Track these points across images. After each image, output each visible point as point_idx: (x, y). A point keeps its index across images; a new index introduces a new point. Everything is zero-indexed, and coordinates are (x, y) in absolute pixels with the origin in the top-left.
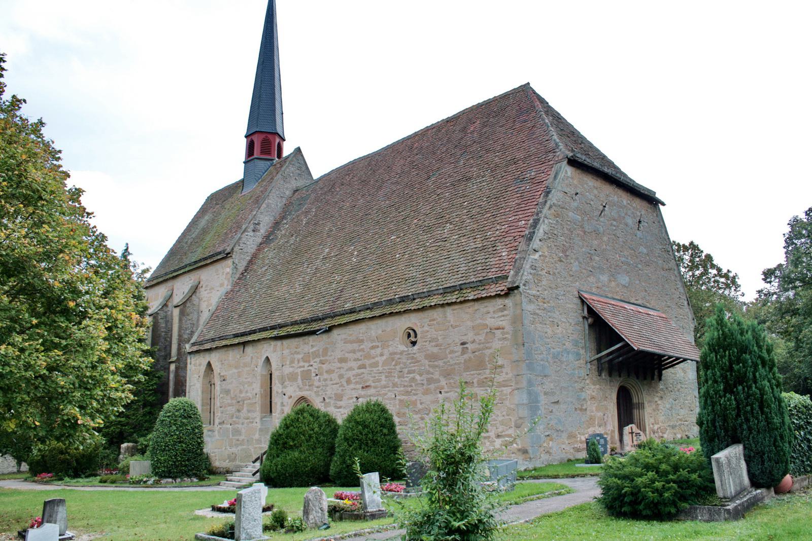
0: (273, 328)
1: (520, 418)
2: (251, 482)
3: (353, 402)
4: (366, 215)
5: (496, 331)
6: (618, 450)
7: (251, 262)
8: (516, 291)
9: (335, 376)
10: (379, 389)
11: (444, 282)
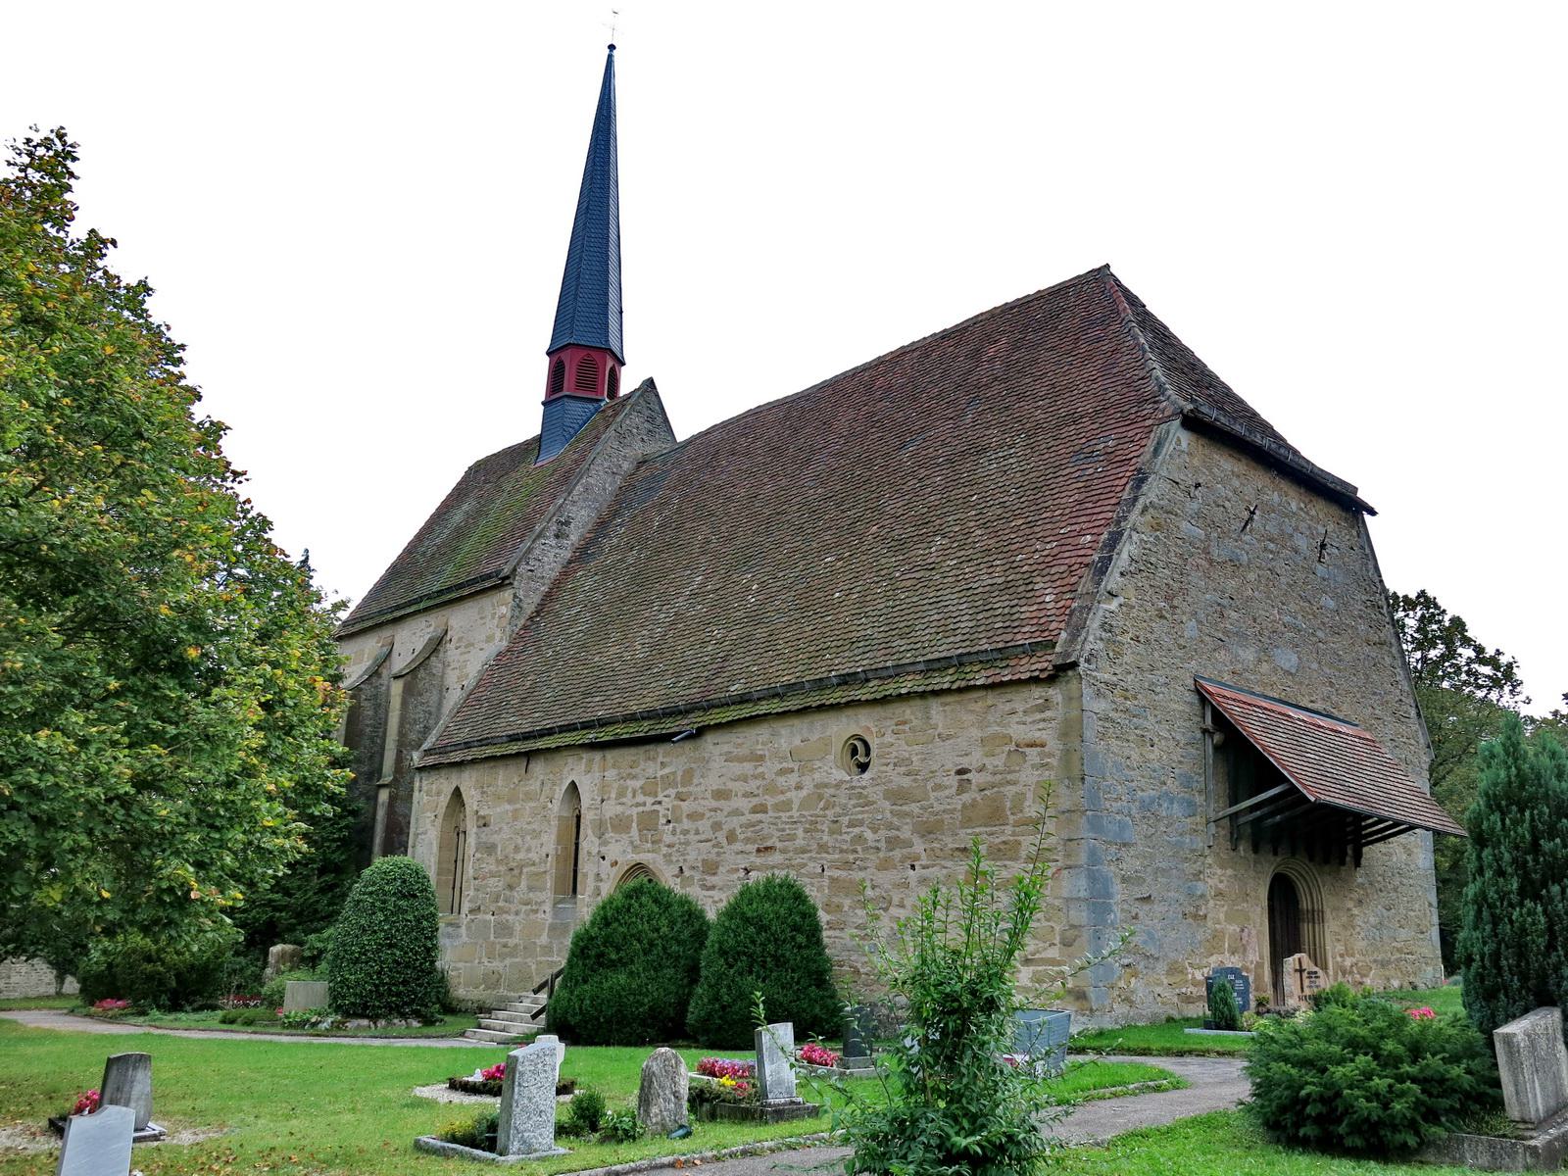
0: (587, 726)
1: (1073, 927)
2: (526, 1031)
3: (739, 879)
4: (778, 513)
5: (1028, 750)
6: (1271, 1006)
7: (548, 597)
8: (1070, 673)
9: (704, 825)
10: (791, 854)
11: (928, 649)
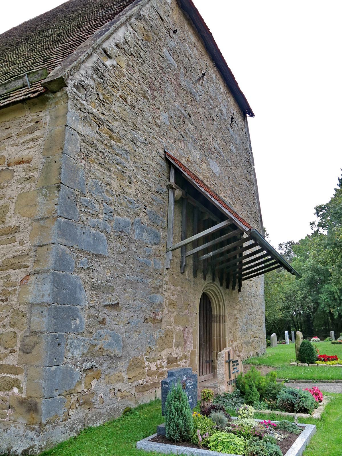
1: (33, 333)
5: (15, 167)
